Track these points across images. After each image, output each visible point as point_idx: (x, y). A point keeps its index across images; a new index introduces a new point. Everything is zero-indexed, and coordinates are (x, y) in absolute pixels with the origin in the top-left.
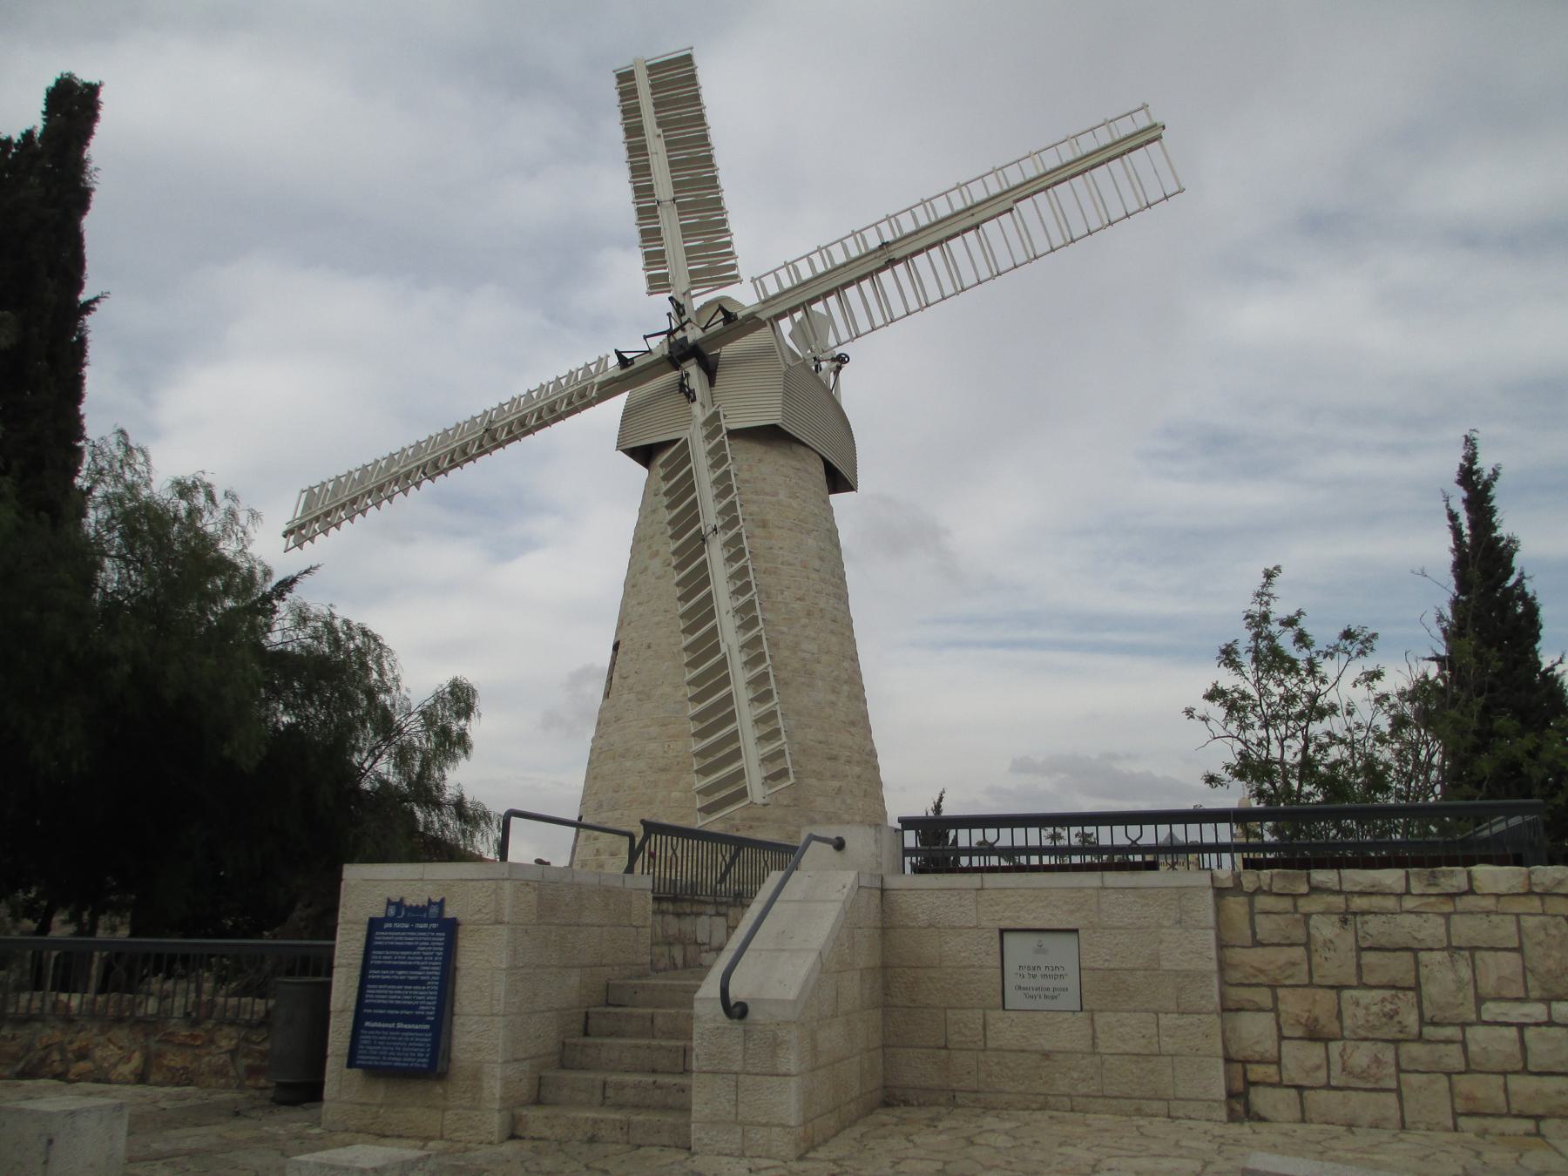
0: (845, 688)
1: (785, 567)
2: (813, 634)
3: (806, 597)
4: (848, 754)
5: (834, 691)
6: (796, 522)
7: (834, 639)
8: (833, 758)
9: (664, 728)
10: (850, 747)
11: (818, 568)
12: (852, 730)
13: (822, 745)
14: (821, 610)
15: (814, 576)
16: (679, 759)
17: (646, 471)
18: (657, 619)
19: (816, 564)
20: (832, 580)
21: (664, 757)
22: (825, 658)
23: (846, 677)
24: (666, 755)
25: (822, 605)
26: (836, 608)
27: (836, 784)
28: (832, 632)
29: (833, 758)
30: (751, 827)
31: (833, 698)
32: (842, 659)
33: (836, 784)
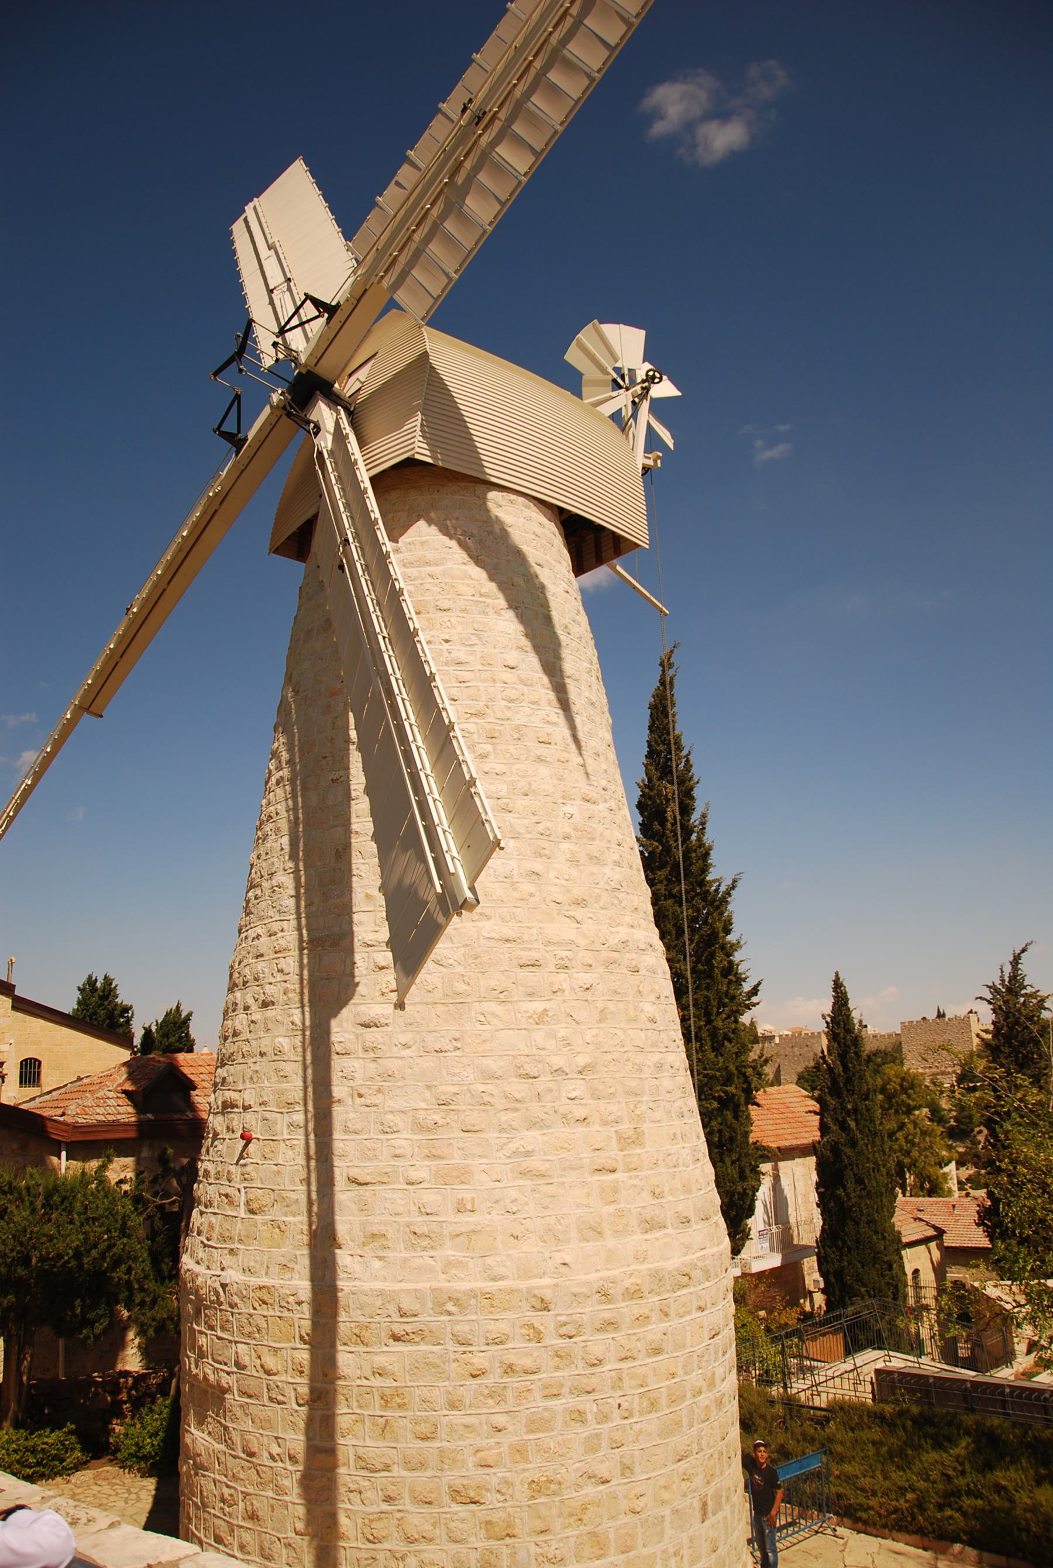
1: (451, 669)
2: (500, 768)
5: (539, 854)
6: (476, 598)
7: (544, 771)
8: (535, 965)
11: (512, 665)
12: (578, 913)
13: (509, 945)
14: (518, 729)
15: (507, 675)
17: (304, 565)
22: (521, 803)
25: (519, 719)
27: (538, 1006)
29: (535, 965)
30: (379, 1091)
31: (538, 867)
33: (538, 1006)
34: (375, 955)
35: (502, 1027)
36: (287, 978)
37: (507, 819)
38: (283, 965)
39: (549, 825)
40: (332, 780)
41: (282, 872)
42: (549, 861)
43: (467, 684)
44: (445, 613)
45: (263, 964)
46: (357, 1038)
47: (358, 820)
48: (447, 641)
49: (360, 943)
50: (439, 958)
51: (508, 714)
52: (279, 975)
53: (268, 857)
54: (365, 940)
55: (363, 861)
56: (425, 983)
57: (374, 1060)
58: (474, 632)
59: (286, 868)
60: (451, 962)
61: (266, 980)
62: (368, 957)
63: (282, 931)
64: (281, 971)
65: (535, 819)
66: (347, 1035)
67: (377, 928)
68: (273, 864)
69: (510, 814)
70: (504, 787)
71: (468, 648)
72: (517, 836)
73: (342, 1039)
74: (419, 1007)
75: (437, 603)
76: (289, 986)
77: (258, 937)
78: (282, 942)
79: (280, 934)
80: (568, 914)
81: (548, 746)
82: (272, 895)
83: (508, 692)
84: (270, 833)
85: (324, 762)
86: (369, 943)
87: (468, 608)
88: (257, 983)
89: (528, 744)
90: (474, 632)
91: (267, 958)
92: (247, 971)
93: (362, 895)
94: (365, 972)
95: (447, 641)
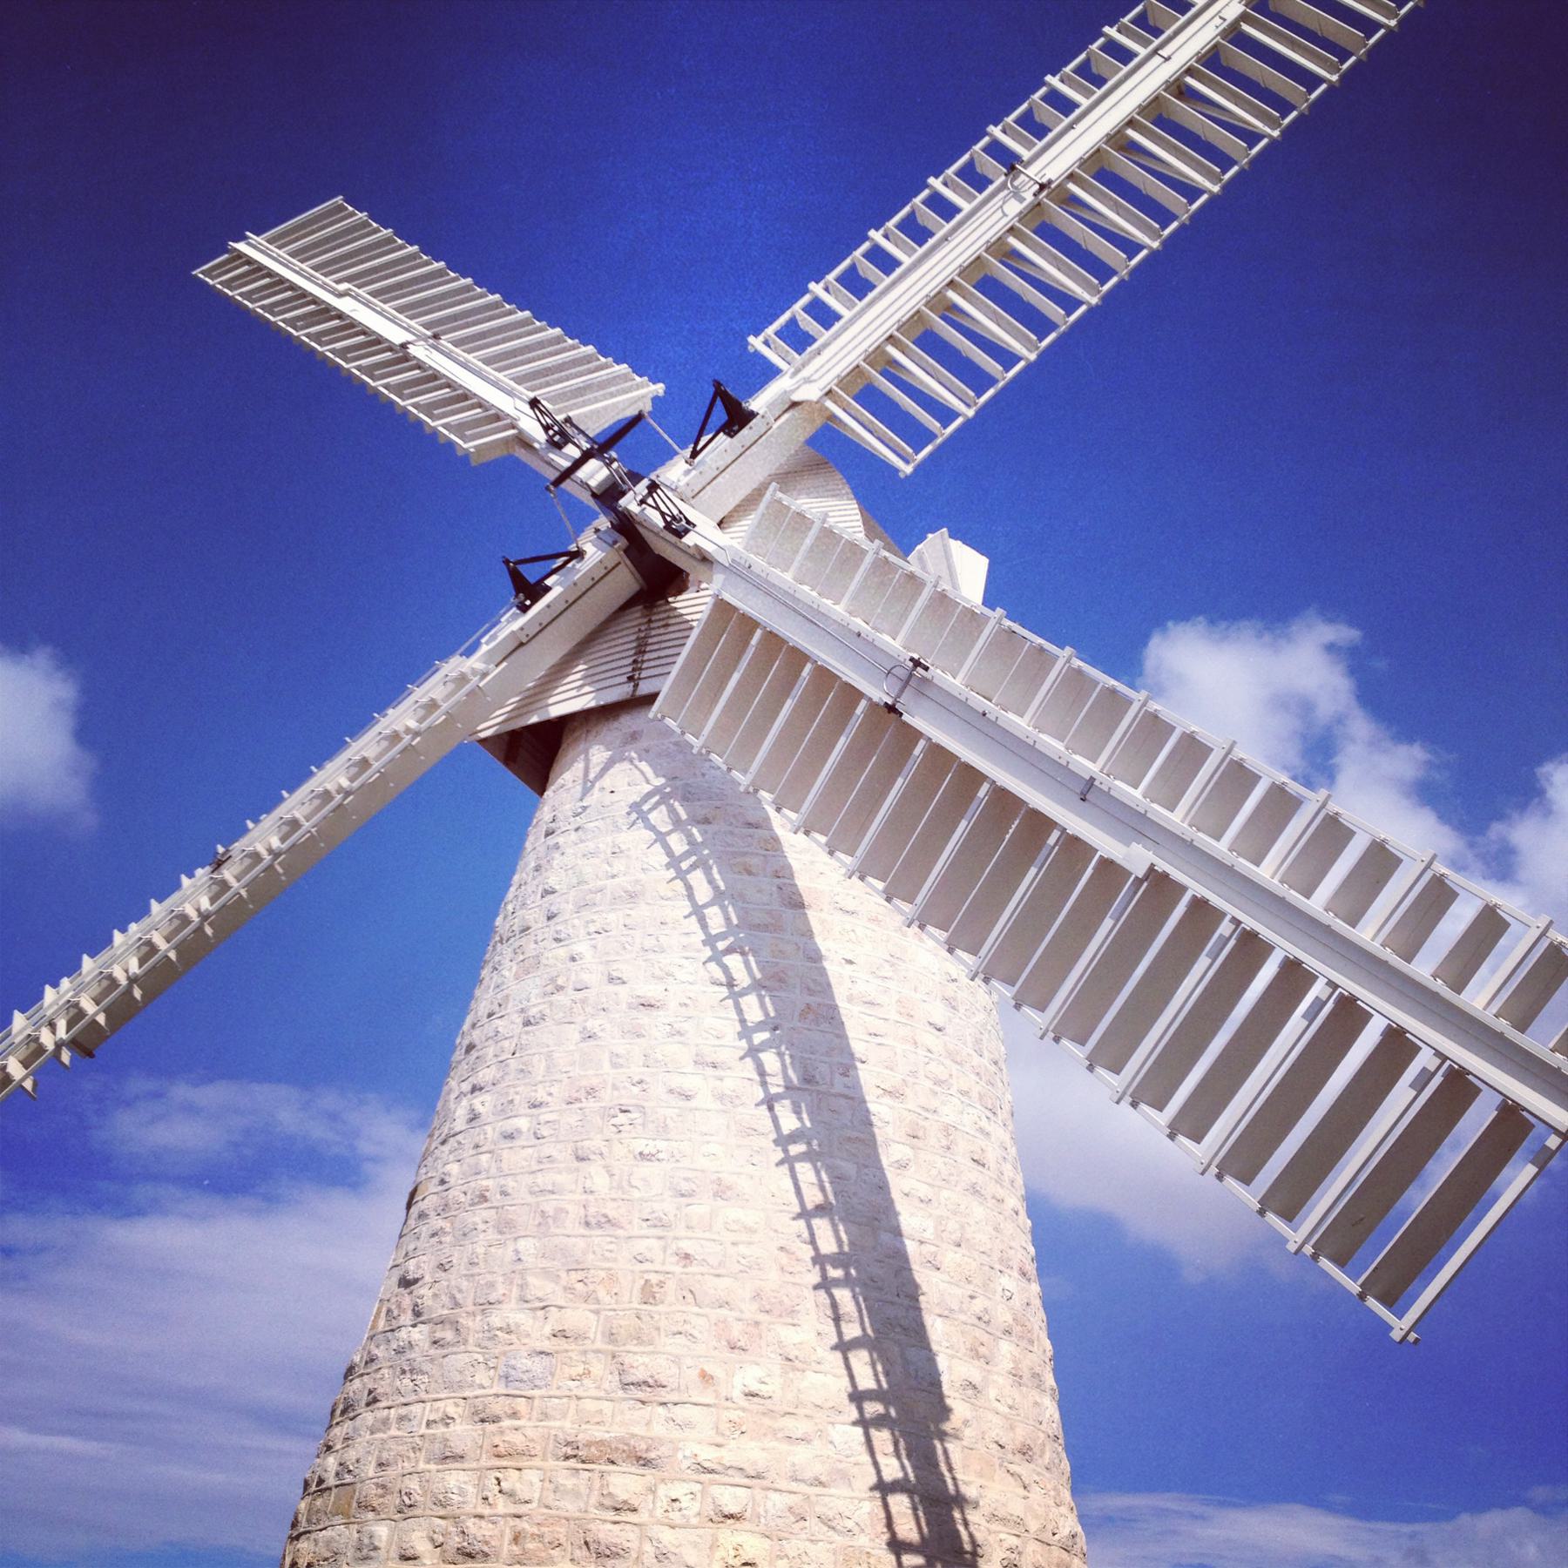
0: (1006, 1347)
3: (908, 1091)
4: (1014, 1541)
7: (978, 1211)
9: (489, 1427)
10: (1019, 1522)
11: (940, 1025)
12: (1023, 1469)
14: (947, 1130)
15: (930, 1039)
16: (523, 1525)
18: (509, 1125)
19: (939, 1014)
20: (976, 1060)
21: (481, 1517)
22: (950, 1257)
23: (1009, 1318)
24: (486, 1511)
26: (981, 1130)
28: (974, 1190)
32: (997, 1266)
34: (716, 1490)
36: (523, 1509)
37: (935, 1280)
38: (511, 1480)
39: (987, 1303)
40: (641, 1154)
41: (513, 1304)
42: (988, 1367)
43: (879, 1040)
44: (847, 918)
45: (462, 1476)
47: (690, 1234)
48: (850, 962)
49: (686, 1463)
50: (831, 1514)
51: (934, 1103)
52: (501, 1500)
53: (476, 1270)
54: (700, 1459)
55: (696, 1309)
56: (805, 1558)
58: (889, 958)
59: (529, 1297)
60: (850, 1524)
61: (468, 1508)
62: (703, 1492)
63: (514, 1415)
64: (511, 1494)
65: (969, 1290)
67: (719, 1440)
68: (491, 1285)
69: (937, 1273)
70: (930, 1224)
71: (879, 982)
72: (946, 1313)
75: (837, 898)
76: (526, 1526)
77: (447, 1420)
78: (517, 1439)
79: (506, 1423)
80: (1013, 1468)
81: (980, 1168)
82: (486, 1343)
83: (933, 1067)
84: (481, 1227)
85: (622, 1118)
86: (706, 1465)
87: (880, 917)
88: (442, 1512)
89: (959, 1158)
90: (889, 958)
91: (474, 1465)
92: (413, 1484)
93: (694, 1373)
94: (694, 1521)
95: (850, 962)
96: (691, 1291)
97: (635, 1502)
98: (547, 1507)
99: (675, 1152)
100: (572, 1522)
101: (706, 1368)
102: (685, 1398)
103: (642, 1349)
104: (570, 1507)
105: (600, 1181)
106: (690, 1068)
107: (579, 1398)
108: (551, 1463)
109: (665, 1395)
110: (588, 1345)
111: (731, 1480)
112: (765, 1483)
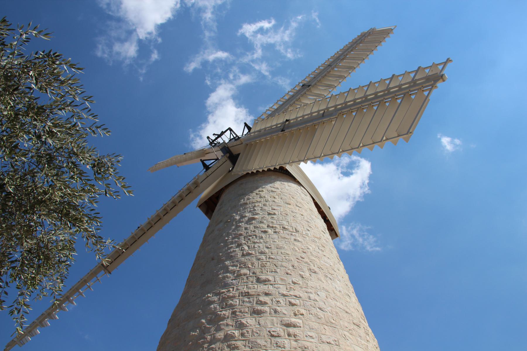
35: (353, 343)
46: (284, 331)
57: (296, 341)
66: (278, 329)
73: (276, 330)
74: (315, 323)
96: (275, 265)
97: (267, 301)
98: (241, 305)
99: (266, 242)
100: (250, 308)
101: (282, 277)
102: (277, 283)
103: (263, 274)
104: (248, 305)
105: (246, 248)
106: (266, 228)
107: (247, 285)
108: (241, 297)
109: (272, 283)
110: (248, 275)
111: (293, 298)
112: (302, 299)
